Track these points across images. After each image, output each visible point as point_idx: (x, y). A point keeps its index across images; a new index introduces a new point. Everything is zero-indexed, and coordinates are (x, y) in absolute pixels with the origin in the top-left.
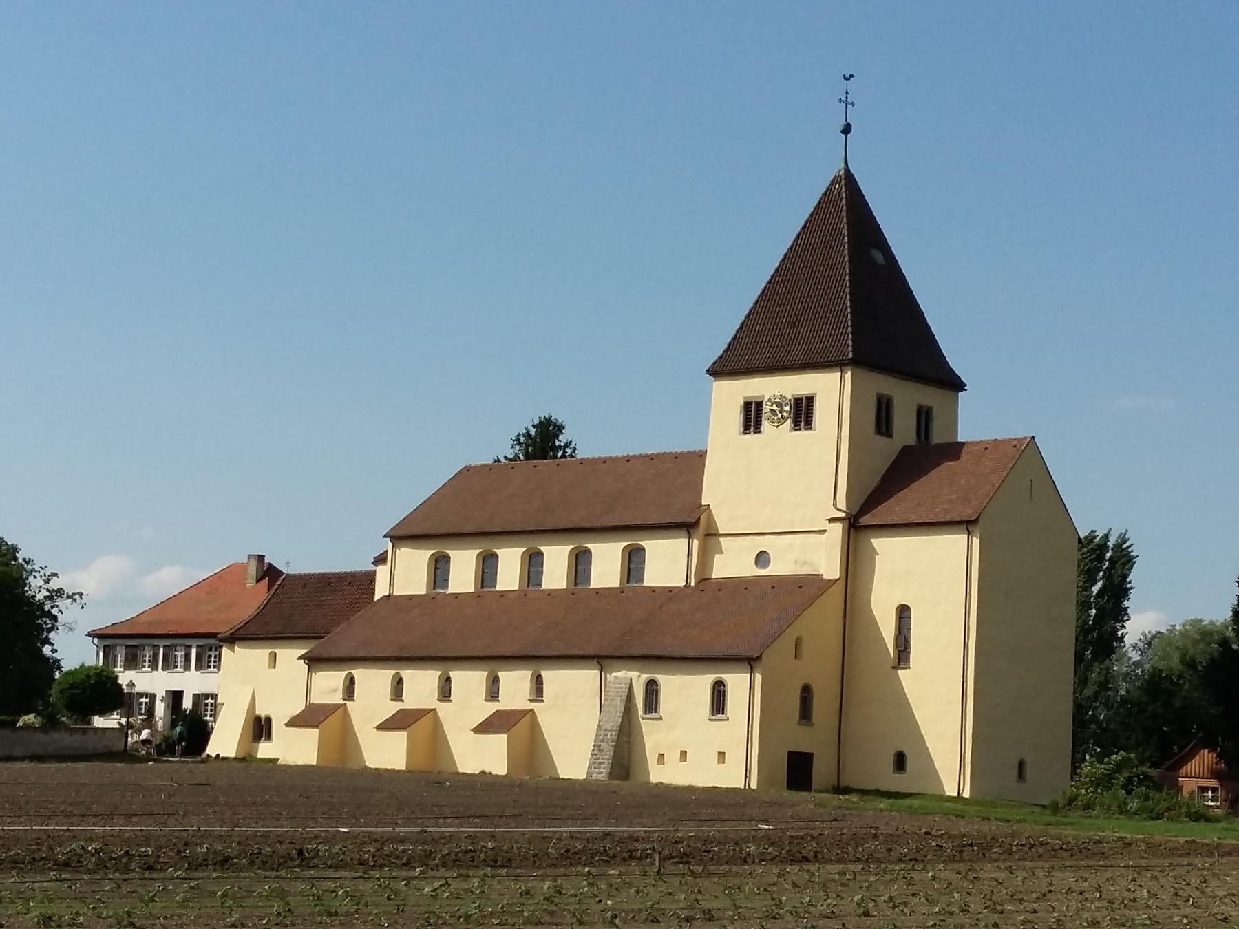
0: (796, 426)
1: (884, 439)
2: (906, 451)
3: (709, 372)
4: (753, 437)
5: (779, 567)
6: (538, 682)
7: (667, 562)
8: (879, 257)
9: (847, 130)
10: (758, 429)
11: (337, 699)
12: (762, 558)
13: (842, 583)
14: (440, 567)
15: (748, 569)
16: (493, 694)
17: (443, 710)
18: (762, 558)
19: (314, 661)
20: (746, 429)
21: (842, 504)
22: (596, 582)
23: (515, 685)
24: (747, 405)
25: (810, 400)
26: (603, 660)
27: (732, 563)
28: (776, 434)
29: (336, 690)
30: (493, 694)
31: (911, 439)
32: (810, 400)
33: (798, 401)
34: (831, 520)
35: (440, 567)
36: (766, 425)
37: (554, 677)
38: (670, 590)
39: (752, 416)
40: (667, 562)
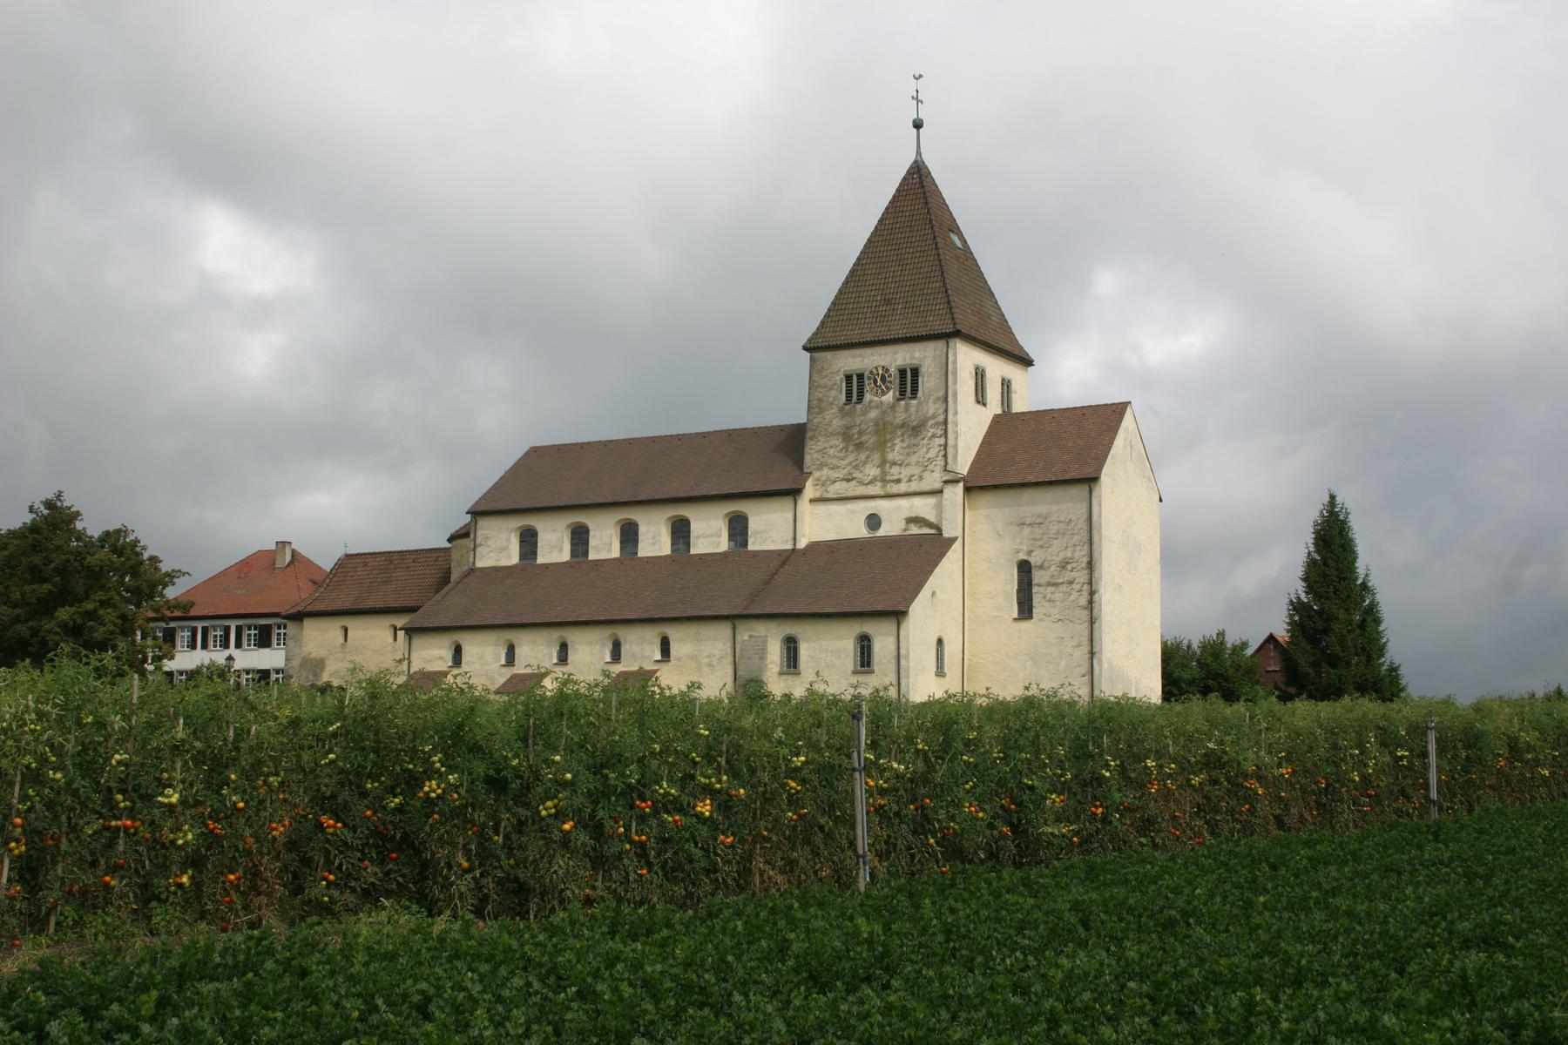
1: (980, 407)
2: (996, 417)
3: (805, 348)
5: (891, 527)
7: (770, 528)
8: (955, 238)
9: (918, 125)
12: (874, 521)
13: (960, 541)
14: (529, 540)
15: (862, 532)
16: (510, 660)
18: (874, 521)
19: (411, 631)
24: (848, 378)
30: (510, 660)
31: (999, 411)
32: (915, 372)
33: (902, 372)
34: (946, 482)
35: (529, 540)
38: (779, 553)
40: (770, 528)
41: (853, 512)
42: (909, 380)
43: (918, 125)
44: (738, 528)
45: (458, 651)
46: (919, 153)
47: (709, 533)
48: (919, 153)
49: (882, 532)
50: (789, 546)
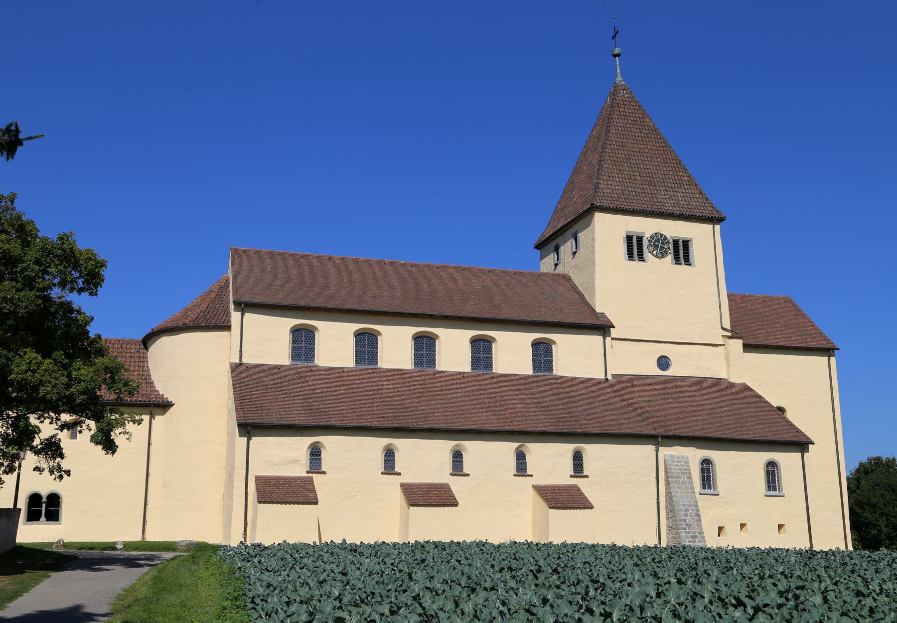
4: (636, 264)
6: (578, 458)
7: (576, 357)
10: (641, 257)
11: (300, 470)
12: (663, 362)
14: (303, 342)
17: (457, 485)
18: (663, 362)
21: (728, 326)
24: (629, 239)
27: (637, 362)
28: (658, 267)
29: (295, 461)
32: (686, 243)
33: (676, 242)
35: (303, 342)
39: (635, 247)
40: (576, 357)
42: (681, 252)
44: (542, 354)
45: (315, 453)
47: (513, 353)
50: (602, 377)
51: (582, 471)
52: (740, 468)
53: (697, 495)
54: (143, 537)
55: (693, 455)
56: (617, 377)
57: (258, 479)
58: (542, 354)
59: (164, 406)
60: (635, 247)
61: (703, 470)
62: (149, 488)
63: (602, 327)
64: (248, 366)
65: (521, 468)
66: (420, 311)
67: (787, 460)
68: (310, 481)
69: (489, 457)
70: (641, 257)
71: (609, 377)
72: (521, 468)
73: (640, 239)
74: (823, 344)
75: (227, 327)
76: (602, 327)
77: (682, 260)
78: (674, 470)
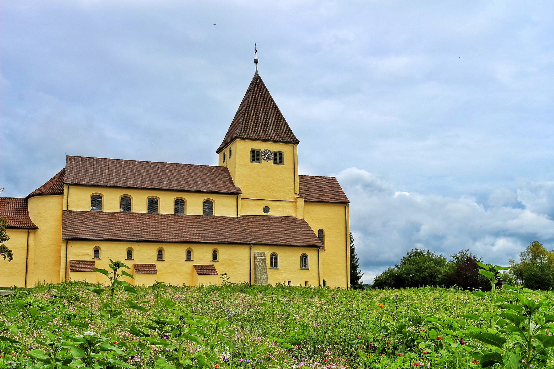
0: (275, 162)
4: (256, 165)
7: (224, 208)
9: (256, 61)
11: (89, 258)
12: (266, 210)
14: (97, 201)
17: (159, 265)
18: (266, 210)
20: (253, 160)
22: (161, 211)
23: (203, 255)
25: (281, 154)
26: (250, 245)
28: (267, 165)
32: (281, 154)
33: (275, 153)
35: (97, 201)
36: (263, 161)
37: (224, 253)
39: (256, 156)
40: (224, 208)
41: (258, 205)
43: (256, 61)
44: (208, 206)
45: (97, 252)
46: (257, 71)
47: (194, 206)
48: (257, 71)
49: (270, 214)
50: (235, 216)
51: (216, 259)
52: (289, 259)
53: (268, 270)
54: (25, 286)
55: (267, 252)
56: (243, 216)
57: (71, 261)
58: (208, 206)
59: (35, 228)
60: (256, 156)
61: (272, 259)
62: (29, 265)
63: (236, 193)
64: (71, 212)
65: (189, 257)
66: (150, 187)
67: (312, 255)
68: (94, 262)
69: (175, 254)
70: (258, 161)
71: (239, 216)
72: (189, 257)
73: (258, 152)
74: (344, 201)
75: (62, 194)
76: (236, 193)
77: (278, 161)
78: (258, 258)
